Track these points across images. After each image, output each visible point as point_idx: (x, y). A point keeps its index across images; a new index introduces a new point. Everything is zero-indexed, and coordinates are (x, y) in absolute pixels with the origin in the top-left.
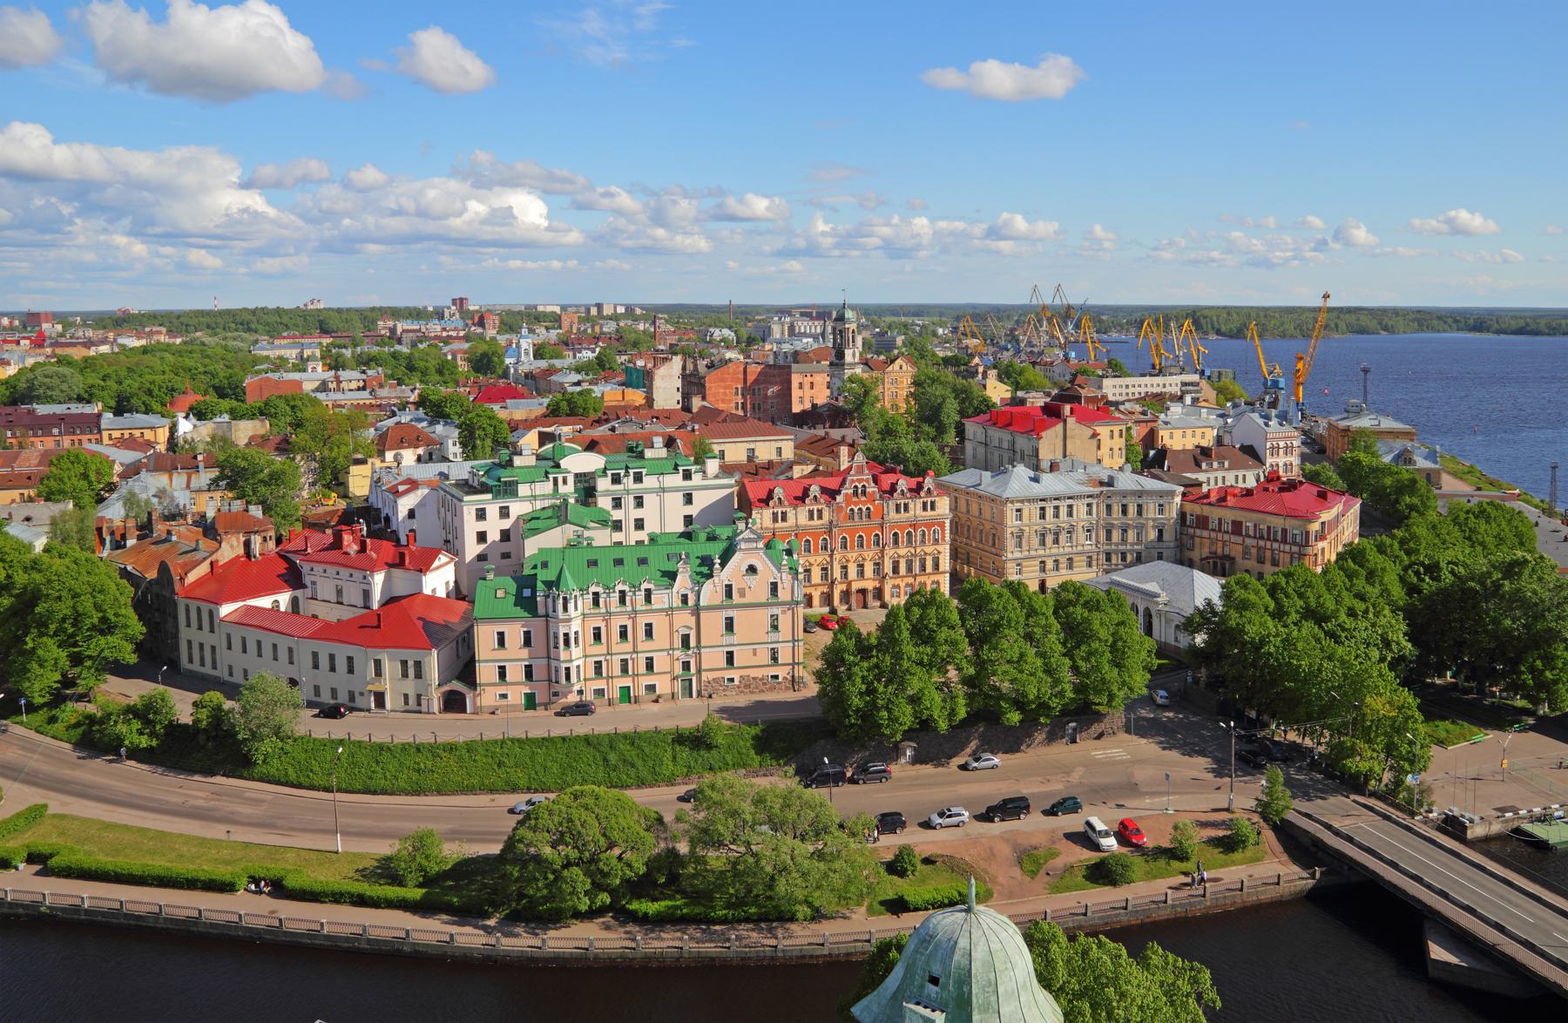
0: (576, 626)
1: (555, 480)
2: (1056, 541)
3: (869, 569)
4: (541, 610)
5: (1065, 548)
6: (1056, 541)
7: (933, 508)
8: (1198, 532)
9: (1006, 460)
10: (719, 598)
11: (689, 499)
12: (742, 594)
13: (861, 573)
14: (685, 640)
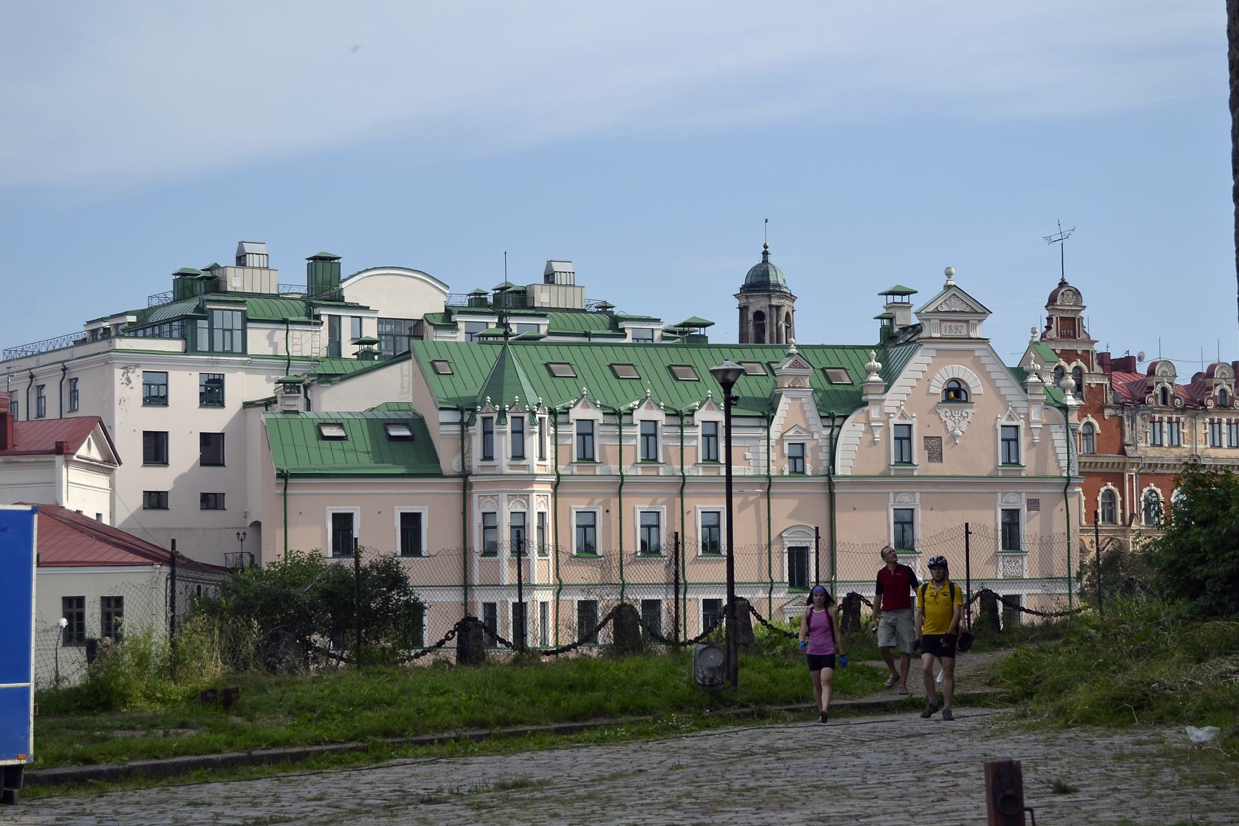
4: (449, 461)
10: (879, 461)
12: (935, 453)
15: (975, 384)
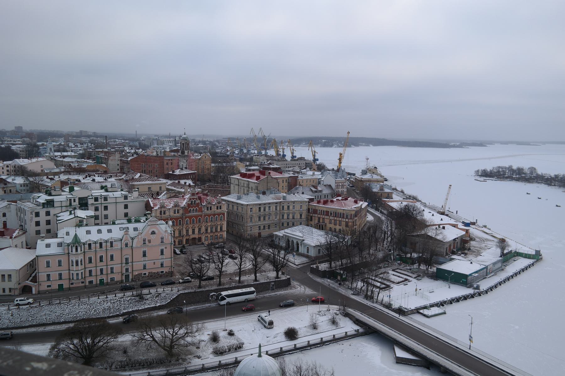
0: (80, 258)
1: (70, 200)
2: (264, 219)
3: (196, 231)
5: (267, 222)
6: (264, 219)
7: (220, 208)
8: (314, 215)
9: (246, 192)
11: (126, 207)
13: (193, 233)
14: (127, 259)
15: (156, 232)
